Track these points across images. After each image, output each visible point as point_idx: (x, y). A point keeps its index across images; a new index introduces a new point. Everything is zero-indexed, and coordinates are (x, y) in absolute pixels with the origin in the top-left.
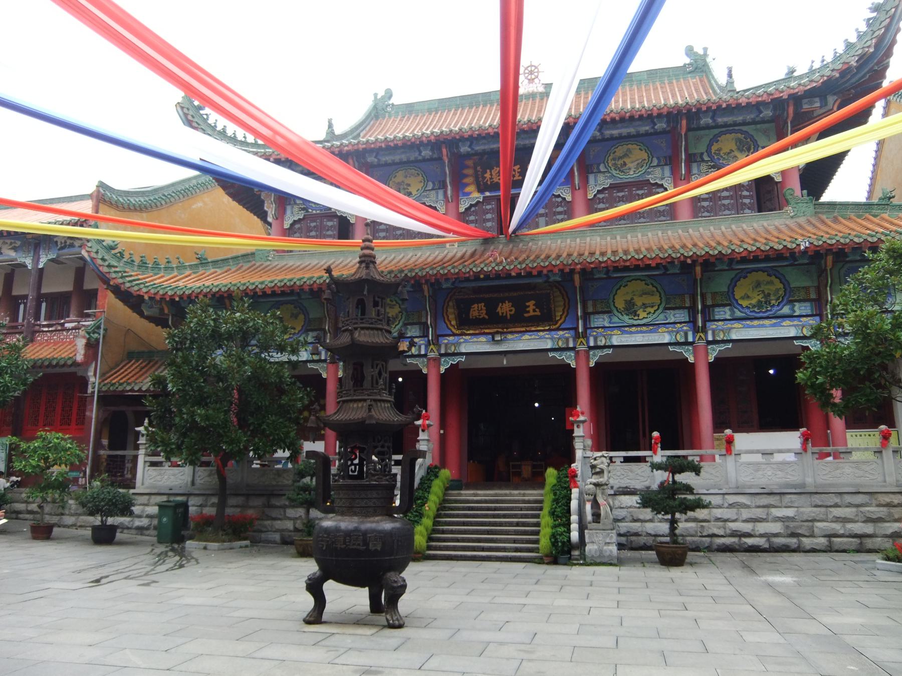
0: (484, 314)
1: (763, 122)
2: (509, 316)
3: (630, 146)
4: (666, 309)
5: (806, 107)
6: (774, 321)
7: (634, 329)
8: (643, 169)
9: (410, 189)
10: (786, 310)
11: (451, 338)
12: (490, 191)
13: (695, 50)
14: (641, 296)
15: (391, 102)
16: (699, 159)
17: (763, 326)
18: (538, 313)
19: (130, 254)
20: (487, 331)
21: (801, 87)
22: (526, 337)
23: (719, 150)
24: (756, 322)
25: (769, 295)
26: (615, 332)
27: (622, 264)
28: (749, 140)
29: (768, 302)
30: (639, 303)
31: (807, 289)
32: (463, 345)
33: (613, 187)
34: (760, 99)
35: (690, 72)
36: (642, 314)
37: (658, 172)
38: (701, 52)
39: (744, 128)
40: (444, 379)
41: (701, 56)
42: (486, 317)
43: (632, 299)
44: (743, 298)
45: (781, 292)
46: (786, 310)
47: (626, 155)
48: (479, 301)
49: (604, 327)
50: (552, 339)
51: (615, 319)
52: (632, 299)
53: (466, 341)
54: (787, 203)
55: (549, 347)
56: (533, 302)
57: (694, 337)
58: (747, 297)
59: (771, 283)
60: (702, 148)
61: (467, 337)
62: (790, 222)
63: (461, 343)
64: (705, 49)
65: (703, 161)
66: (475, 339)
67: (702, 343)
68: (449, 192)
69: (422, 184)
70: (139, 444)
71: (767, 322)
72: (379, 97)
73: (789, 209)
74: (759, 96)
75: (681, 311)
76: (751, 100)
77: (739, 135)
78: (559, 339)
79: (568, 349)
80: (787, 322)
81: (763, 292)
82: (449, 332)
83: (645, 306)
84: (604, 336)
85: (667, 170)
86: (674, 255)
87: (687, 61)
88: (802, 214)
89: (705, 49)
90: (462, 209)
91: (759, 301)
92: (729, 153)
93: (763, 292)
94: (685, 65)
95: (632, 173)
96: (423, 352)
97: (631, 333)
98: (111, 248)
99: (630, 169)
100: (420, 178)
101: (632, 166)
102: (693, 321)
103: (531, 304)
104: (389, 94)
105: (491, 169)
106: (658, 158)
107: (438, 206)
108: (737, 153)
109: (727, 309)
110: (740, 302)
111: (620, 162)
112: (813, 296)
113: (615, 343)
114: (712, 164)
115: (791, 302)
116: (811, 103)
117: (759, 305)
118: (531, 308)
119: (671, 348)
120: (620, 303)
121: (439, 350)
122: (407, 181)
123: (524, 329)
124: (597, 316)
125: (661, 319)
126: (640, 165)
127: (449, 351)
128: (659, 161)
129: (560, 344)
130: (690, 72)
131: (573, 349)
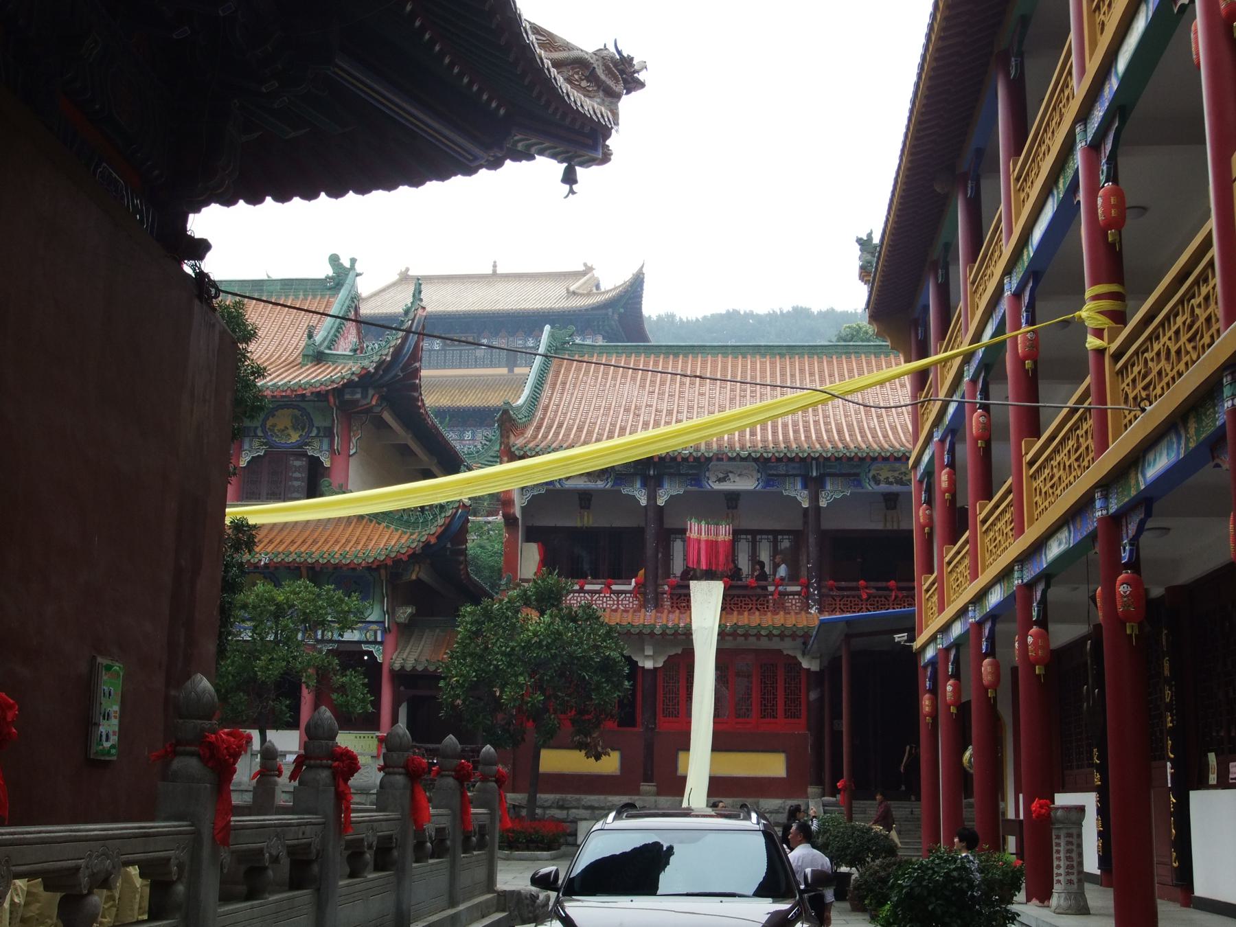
5: (347, 397)
21: (323, 387)
23: (274, 425)
34: (284, 394)
35: (330, 289)
38: (347, 264)
41: (345, 268)
64: (353, 261)
65: (256, 436)
74: (283, 391)
76: (275, 394)
77: (296, 411)
87: (330, 273)
89: (353, 261)
92: (283, 431)
114: (265, 441)
116: (353, 393)
130: (330, 289)
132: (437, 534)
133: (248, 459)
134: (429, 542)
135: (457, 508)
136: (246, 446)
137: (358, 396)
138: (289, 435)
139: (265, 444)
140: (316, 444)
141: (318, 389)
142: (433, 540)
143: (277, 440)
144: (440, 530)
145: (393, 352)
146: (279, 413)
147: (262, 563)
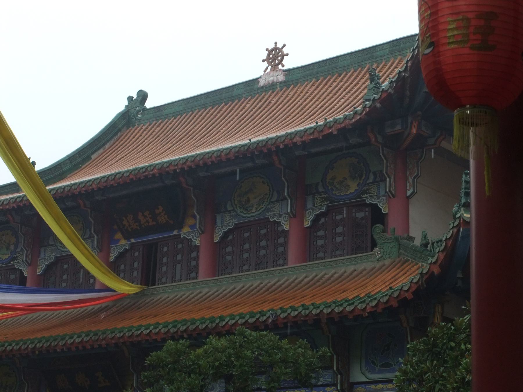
12: (134, 238)
28: (362, 164)
33: (237, 227)
65: (318, 193)
68: (95, 242)
76: (304, 139)
88: (388, 256)
90: (112, 259)
95: (254, 211)
99: (252, 206)
132: (439, 262)
133: (312, 217)
134: (433, 272)
135: (459, 226)
136: (309, 205)
137: (399, 127)
138: (348, 186)
139: (326, 199)
141: (343, 125)
142: (436, 270)
143: (336, 193)
144: (442, 256)
145: (411, 66)
147: (270, 320)
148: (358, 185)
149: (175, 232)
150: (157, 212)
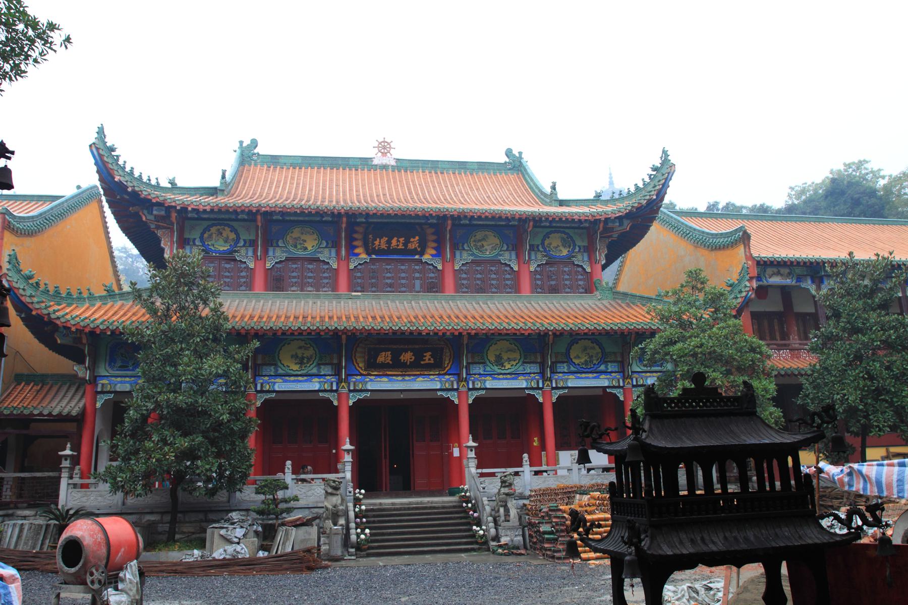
0: (389, 361)
1: (582, 228)
2: (408, 363)
3: (487, 233)
4: (524, 362)
6: (595, 375)
7: (501, 376)
8: (496, 252)
9: (306, 245)
10: (602, 367)
11: (359, 377)
12: (376, 255)
13: (514, 152)
14: (507, 352)
15: (256, 151)
16: (536, 249)
17: (588, 378)
18: (432, 362)
19: (45, 284)
20: (388, 373)
22: (421, 379)
23: (550, 244)
24: (583, 375)
25: (592, 356)
26: (488, 378)
27: (505, 332)
29: (591, 361)
30: (505, 358)
31: (615, 353)
32: (370, 383)
35: (510, 169)
36: (508, 366)
37: (507, 255)
39: (567, 231)
40: (351, 409)
42: (391, 362)
43: (500, 354)
44: (575, 358)
45: (600, 355)
46: (602, 367)
47: (484, 239)
48: (386, 350)
49: (480, 374)
50: (440, 381)
51: (488, 369)
52: (500, 354)
53: (371, 380)
54: (597, 289)
55: (438, 387)
56: (430, 353)
57: (543, 385)
58: (578, 357)
59: (593, 348)
60: (538, 241)
61: (372, 377)
62: (598, 303)
63: (367, 382)
65: (539, 250)
66: (379, 379)
67: (549, 388)
69: (317, 242)
70: (61, 468)
71: (590, 375)
72: (245, 145)
73: (597, 293)
75: (535, 365)
77: (563, 235)
78: (446, 381)
79: (453, 390)
80: (603, 376)
81: (588, 354)
82: (358, 373)
83: (509, 360)
84: (480, 381)
85: (513, 254)
86: (540, 328)
89: (520, 153)
91: (586, 361)
93: (588, 354)
94: (506, 163)
96: (334, 388)
97: (499, 379)
98: (30, 277)
99: (486, 250)
100: (315, 236)
101: (489, 248)
102: (542, 373)
103: (428, 355)
104: (254, 143)
105: (381, 238)
106: (507, 245)
107: (331, 262)
108: (561, 248)
109: (565, 365)
110: (574, 360)
111: (480, 244)
112: (619, 359)
113: (488, 386)
115: (606, 363)
117: (586, 363)
118: (428, 358)
119: (527, 392)
120: (492, 358)
121: (349, 387)
122: (303, 237)
123: (418, 373)
124: (475, 366)
125: (520, 370)
126: (494, 248)
127: (357, 388)
128: (508, 248)
129: (447, 386)
130: (510, 169)
131: (457, 390)
139: (545, 256)
140: (580, 257)
146: (552, 235)
148: (569, 251)
149: (417, 257)
150: (412, 240)
